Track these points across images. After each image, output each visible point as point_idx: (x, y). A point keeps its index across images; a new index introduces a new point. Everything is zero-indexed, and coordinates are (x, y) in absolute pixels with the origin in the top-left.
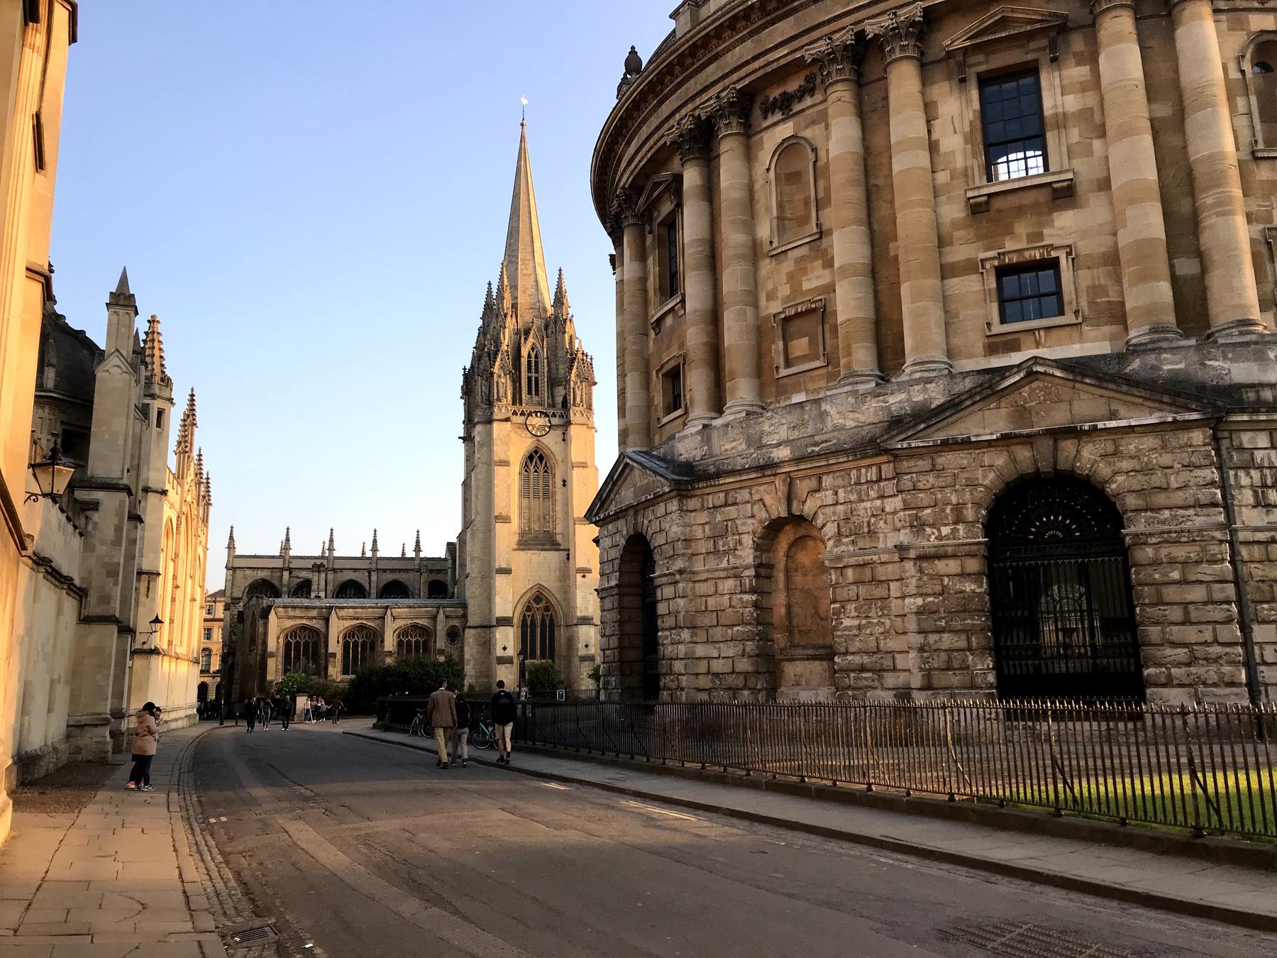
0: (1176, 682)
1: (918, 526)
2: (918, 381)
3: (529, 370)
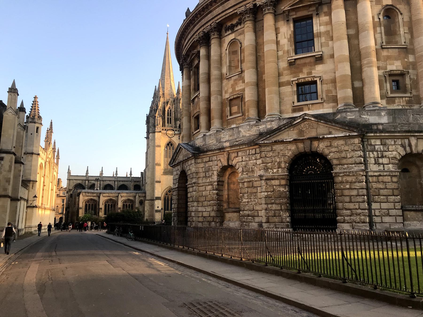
0: (346, 222)
1: (266, 169)
2: (269, 121)
3: (168, 115)
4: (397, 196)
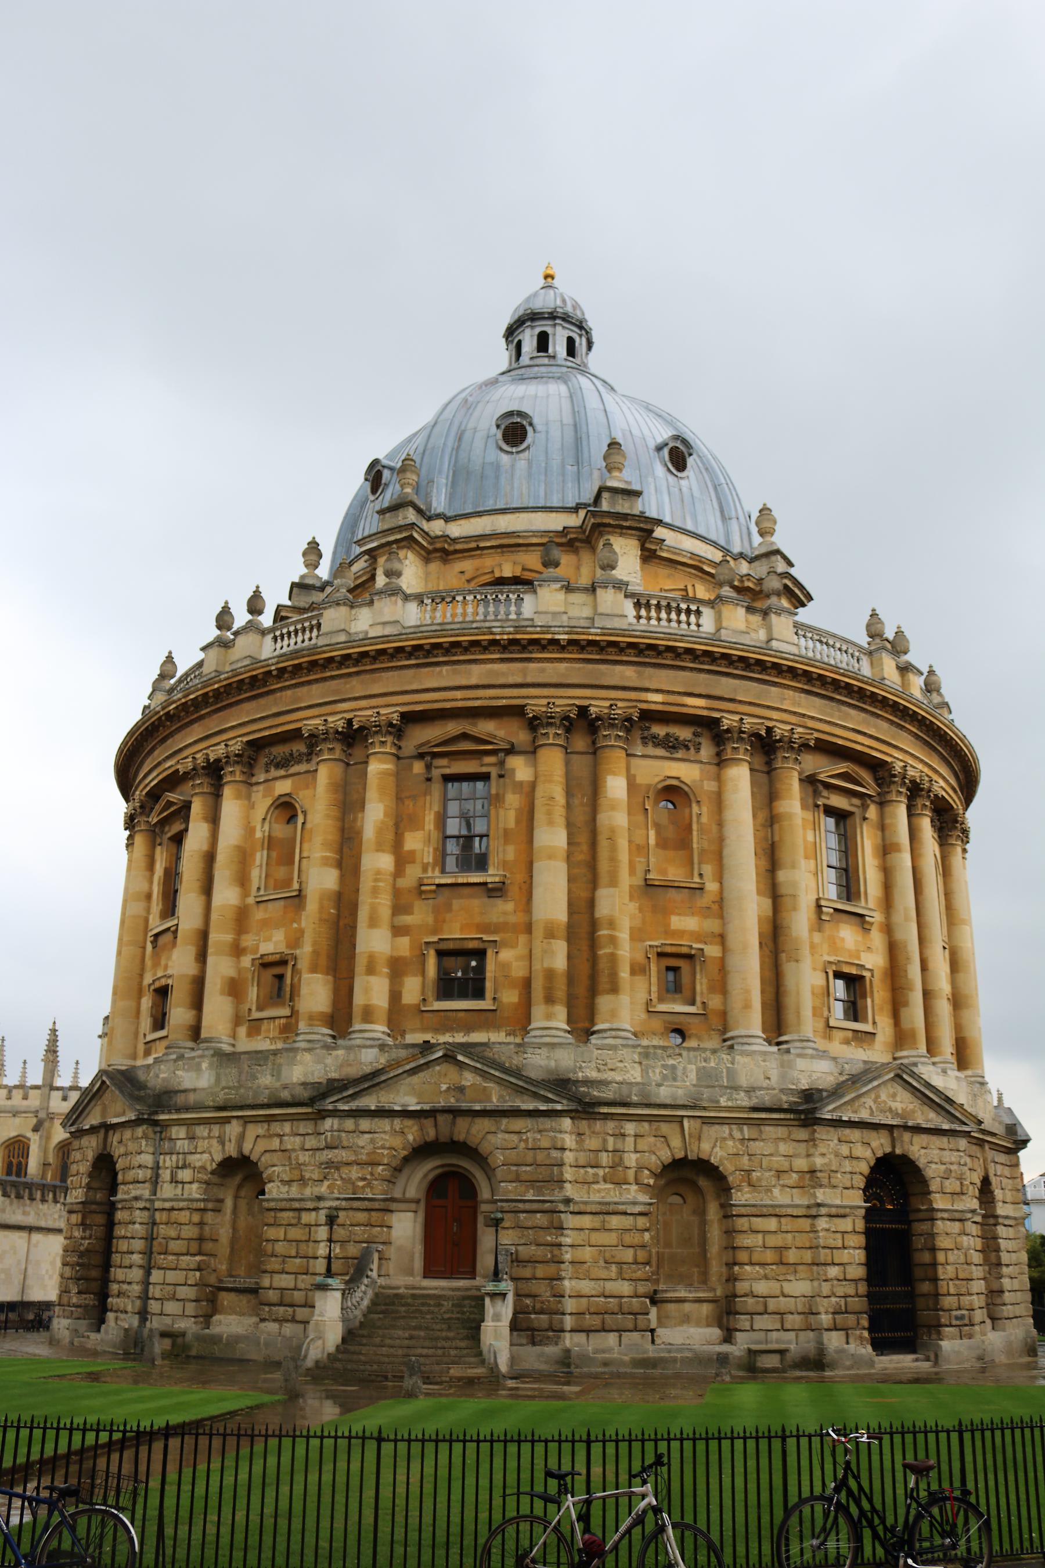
4: (195, 1255)
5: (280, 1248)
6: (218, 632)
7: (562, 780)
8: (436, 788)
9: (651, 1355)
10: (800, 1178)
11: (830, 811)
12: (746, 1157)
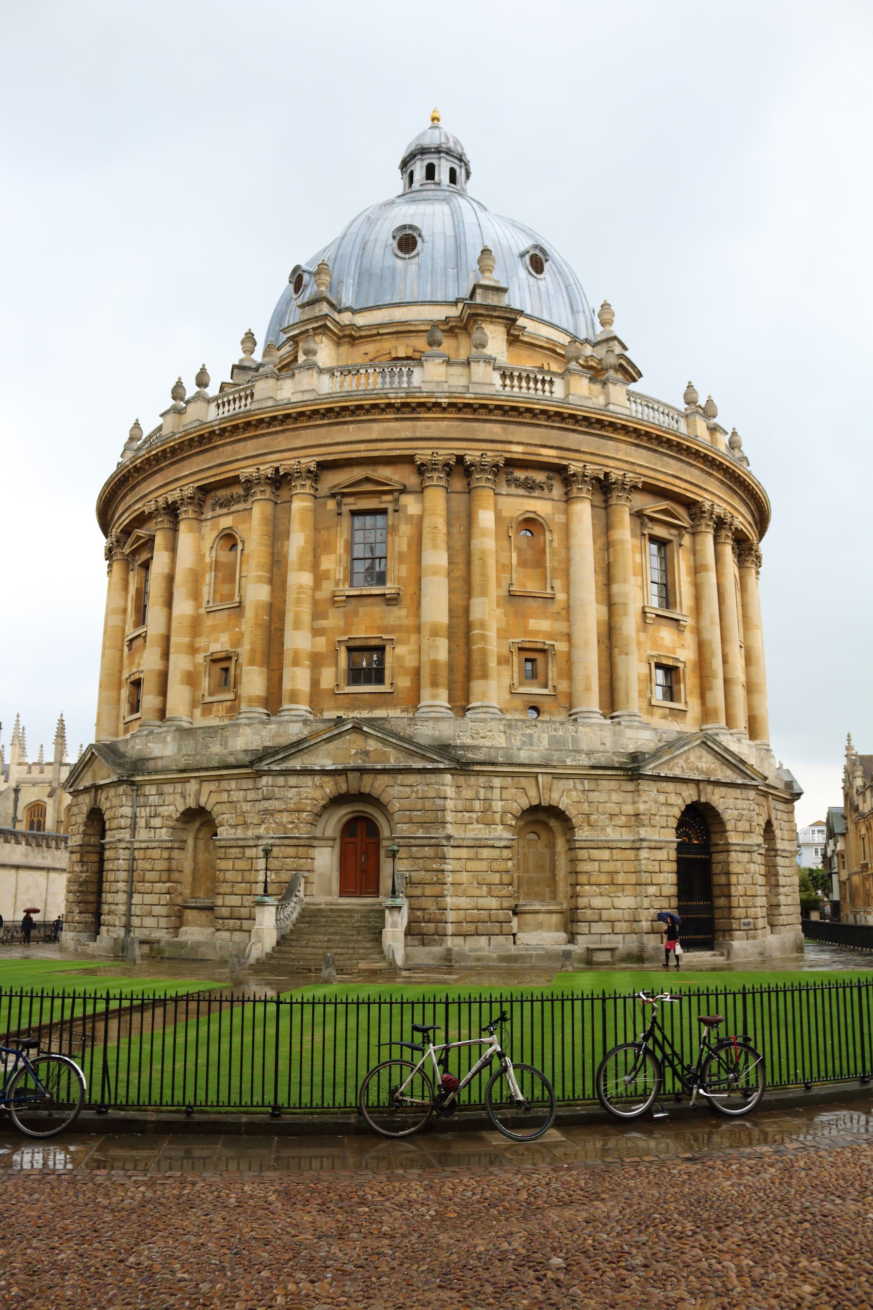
5: (230, 876)
6: (173, 402)
7: (444, 513)
8: (346, 520)
9: (513, 952)
10: (628, 820)
11: (653, 539)
12: (586, 804)
